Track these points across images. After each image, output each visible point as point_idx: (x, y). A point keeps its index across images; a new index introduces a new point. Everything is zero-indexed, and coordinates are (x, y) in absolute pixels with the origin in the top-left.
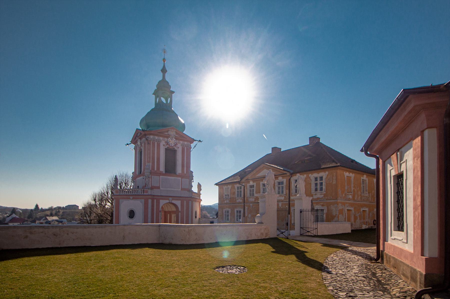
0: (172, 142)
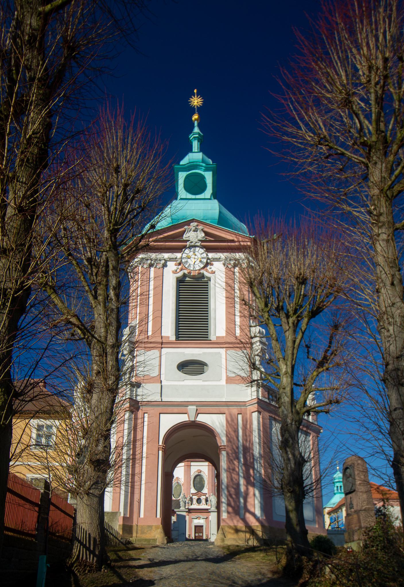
0: (194, 259)
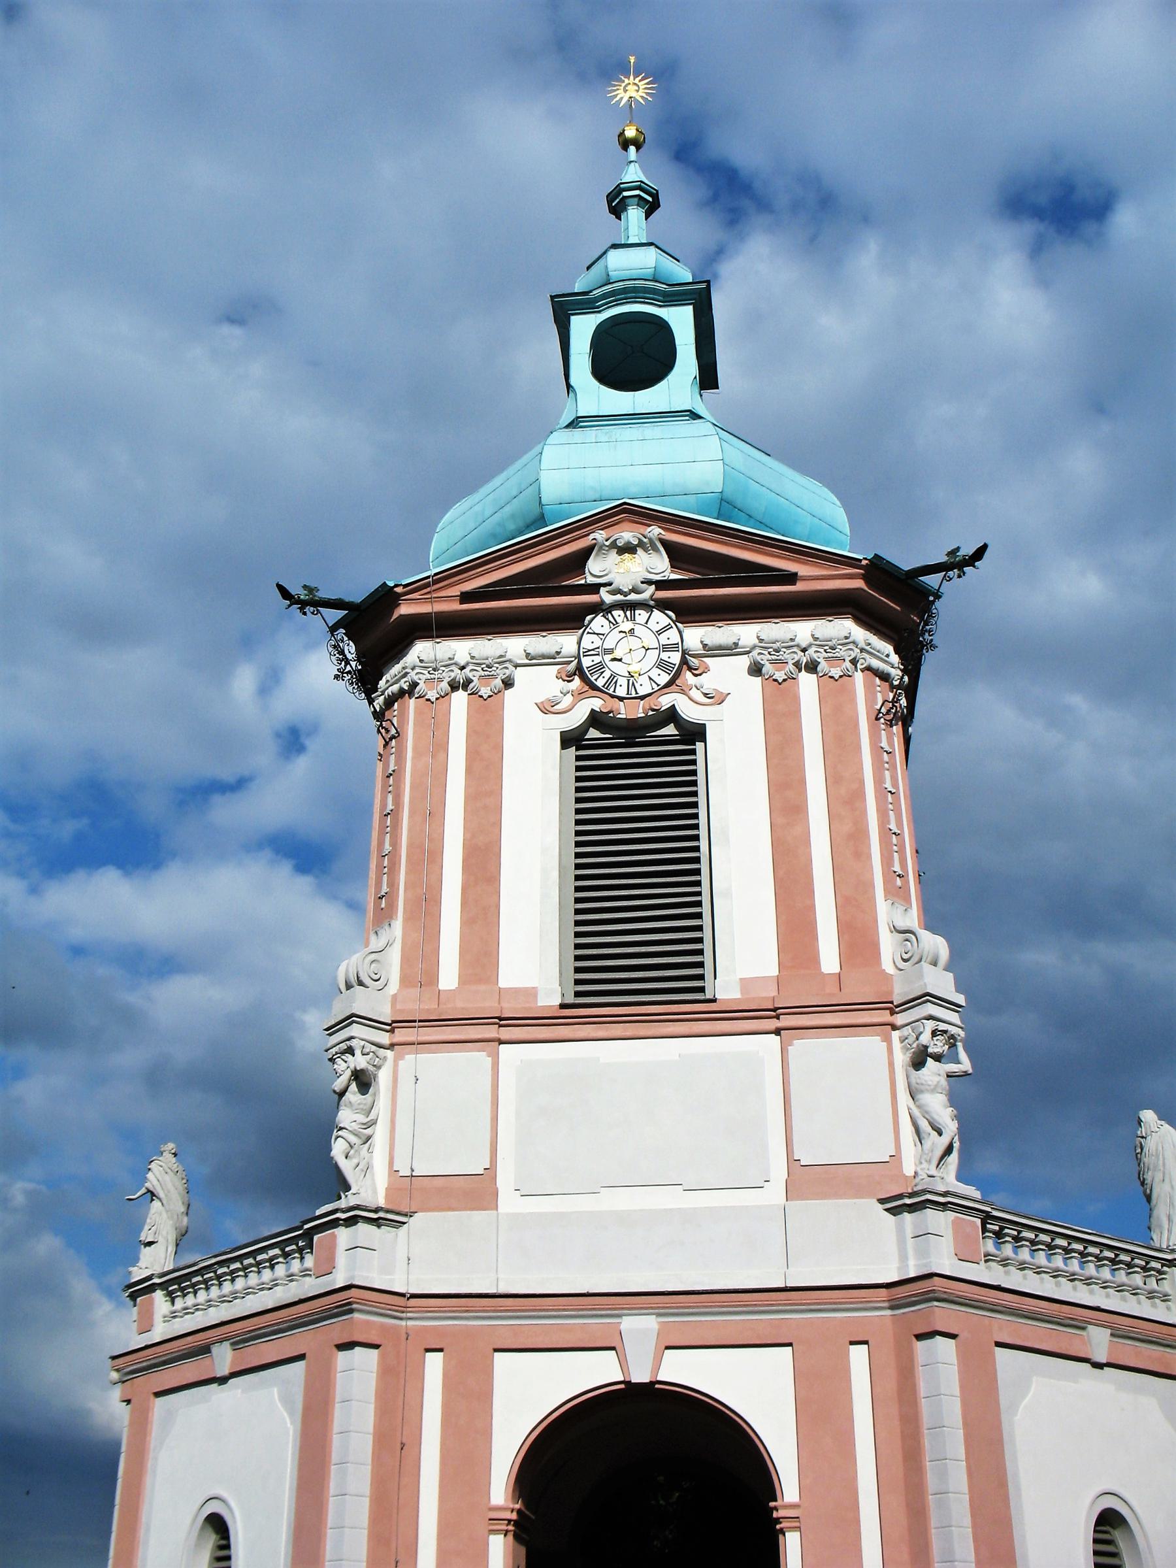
0: (634, 652)
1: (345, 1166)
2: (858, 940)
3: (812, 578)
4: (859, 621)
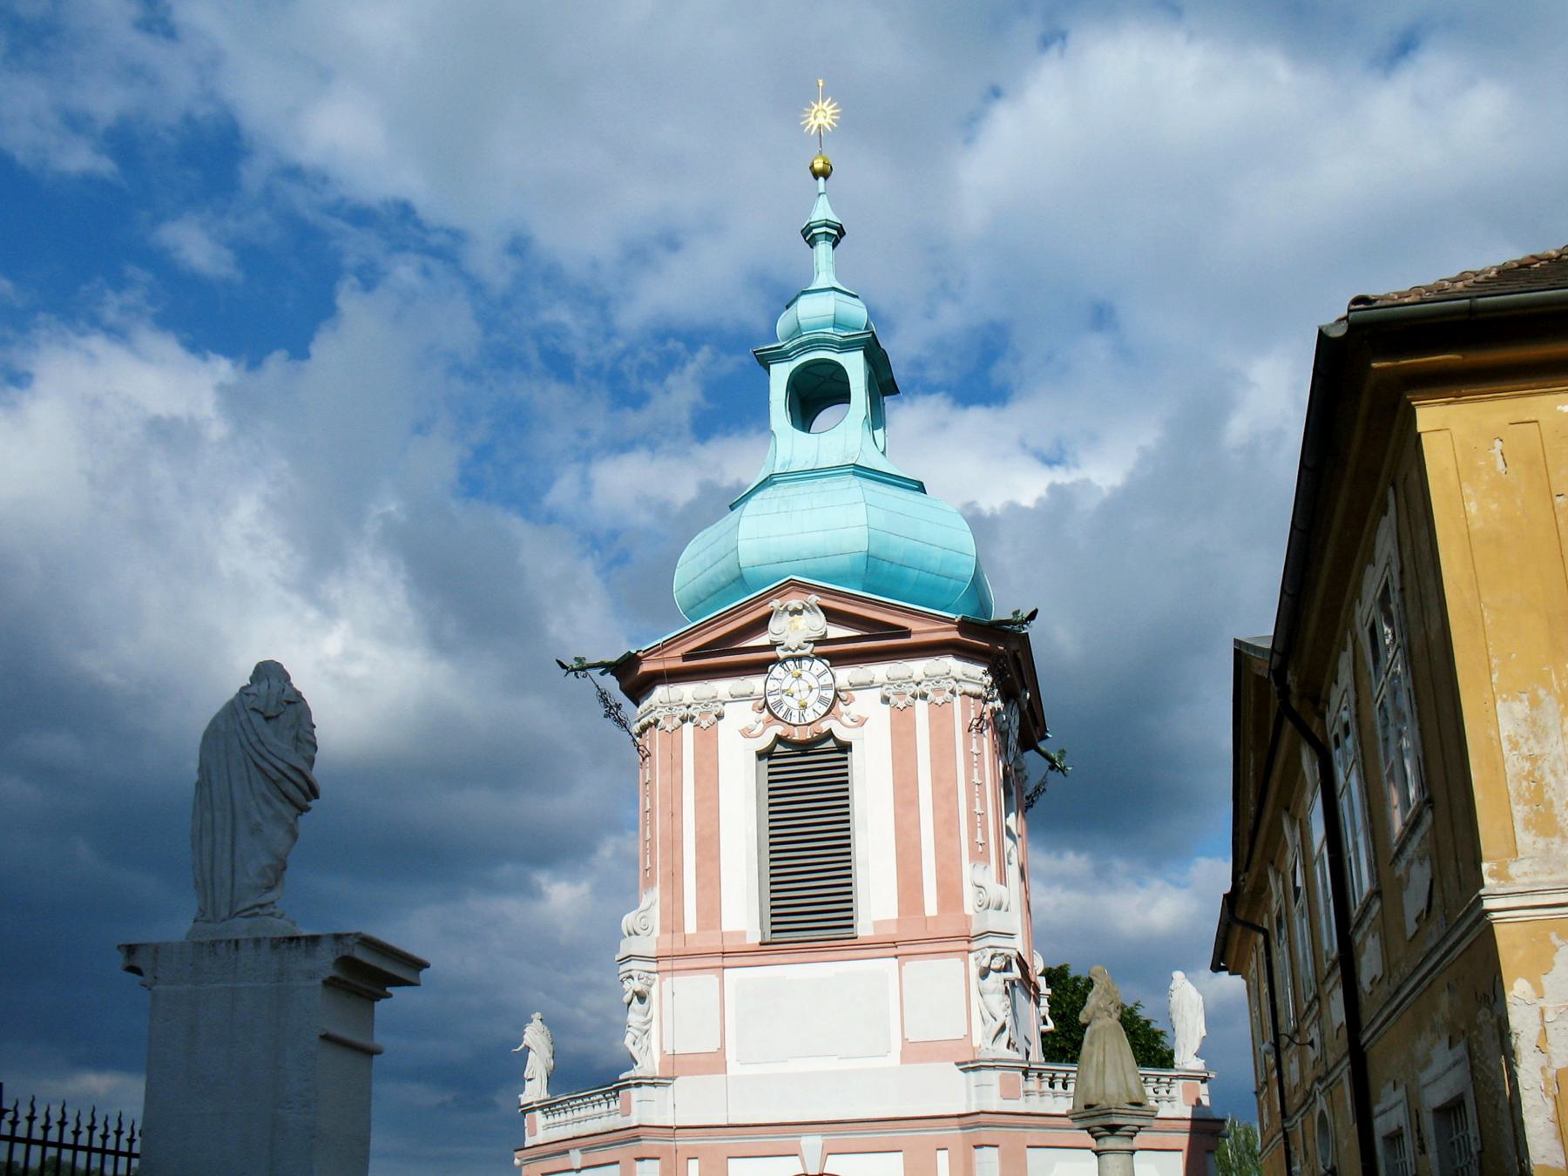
0: (802, 692)
1: (634, 1050)
2: (950, 894)
3: (922, 632)
4: (957, 656)
